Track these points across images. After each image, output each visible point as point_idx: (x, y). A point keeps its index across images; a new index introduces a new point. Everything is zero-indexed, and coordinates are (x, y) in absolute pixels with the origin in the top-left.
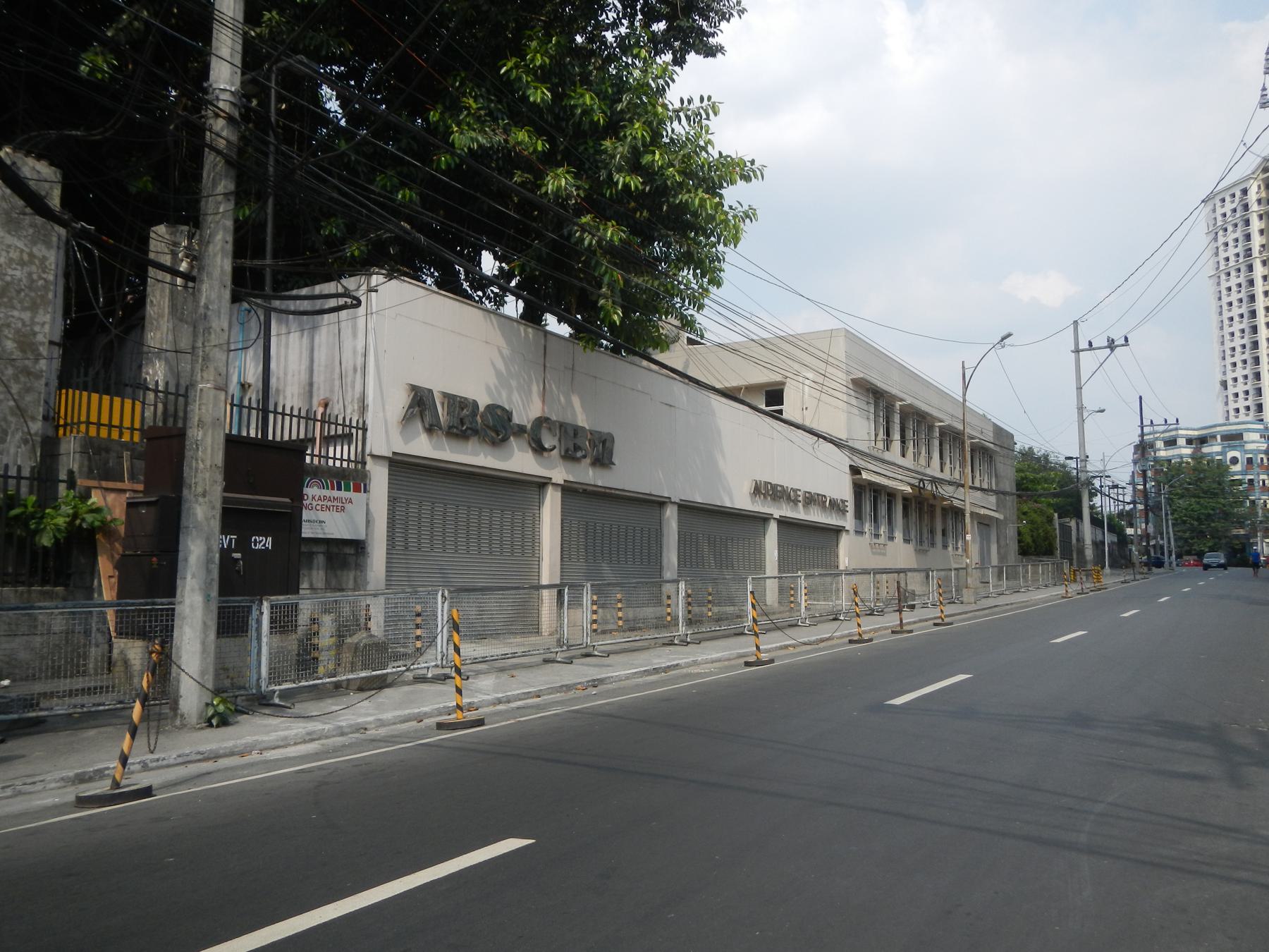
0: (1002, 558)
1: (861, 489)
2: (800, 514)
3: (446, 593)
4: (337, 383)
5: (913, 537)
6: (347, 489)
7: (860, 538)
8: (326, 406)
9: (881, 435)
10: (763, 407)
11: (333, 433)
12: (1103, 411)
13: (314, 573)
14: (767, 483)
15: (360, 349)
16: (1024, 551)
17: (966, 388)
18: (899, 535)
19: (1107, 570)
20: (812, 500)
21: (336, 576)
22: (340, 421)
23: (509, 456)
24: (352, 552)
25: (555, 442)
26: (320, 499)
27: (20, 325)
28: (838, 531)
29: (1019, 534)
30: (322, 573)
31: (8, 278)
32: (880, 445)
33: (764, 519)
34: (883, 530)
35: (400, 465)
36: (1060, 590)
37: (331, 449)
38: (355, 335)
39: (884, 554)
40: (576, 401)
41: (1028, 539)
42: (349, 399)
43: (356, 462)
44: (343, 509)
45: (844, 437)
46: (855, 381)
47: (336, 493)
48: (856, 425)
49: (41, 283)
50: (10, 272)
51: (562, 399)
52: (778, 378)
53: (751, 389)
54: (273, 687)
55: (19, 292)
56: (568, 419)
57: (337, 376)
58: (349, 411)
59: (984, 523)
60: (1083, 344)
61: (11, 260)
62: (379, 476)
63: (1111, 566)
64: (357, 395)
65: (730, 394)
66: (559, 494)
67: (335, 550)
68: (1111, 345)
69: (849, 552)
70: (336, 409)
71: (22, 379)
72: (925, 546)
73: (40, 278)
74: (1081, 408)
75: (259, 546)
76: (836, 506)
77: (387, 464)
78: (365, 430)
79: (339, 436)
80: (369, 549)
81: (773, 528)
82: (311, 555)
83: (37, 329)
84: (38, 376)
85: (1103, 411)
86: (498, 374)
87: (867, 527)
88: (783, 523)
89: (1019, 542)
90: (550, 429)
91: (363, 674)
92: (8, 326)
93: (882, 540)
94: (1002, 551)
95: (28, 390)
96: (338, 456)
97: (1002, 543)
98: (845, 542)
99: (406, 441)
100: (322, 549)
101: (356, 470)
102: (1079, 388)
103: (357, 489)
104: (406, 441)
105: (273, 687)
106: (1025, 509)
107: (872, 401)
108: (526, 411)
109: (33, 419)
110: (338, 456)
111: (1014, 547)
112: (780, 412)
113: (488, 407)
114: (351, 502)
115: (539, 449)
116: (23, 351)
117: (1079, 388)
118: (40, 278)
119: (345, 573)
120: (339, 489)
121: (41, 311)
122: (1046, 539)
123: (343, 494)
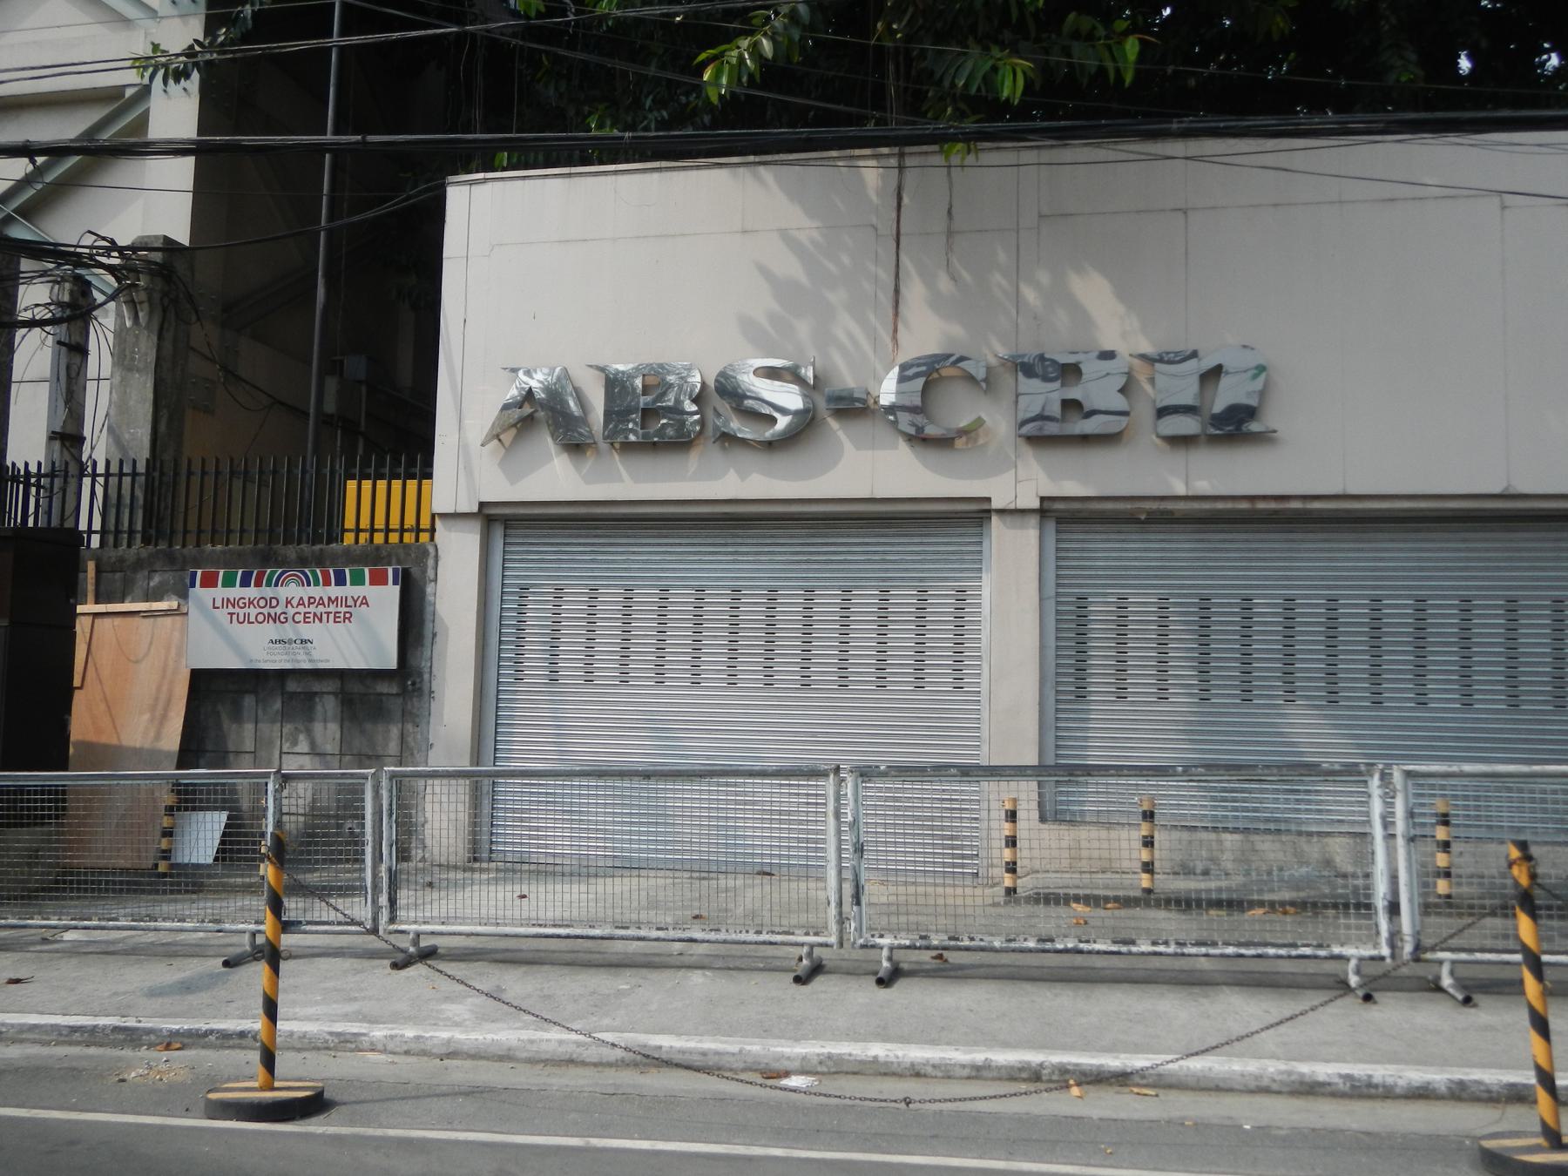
6: (358, 580)
13: (318, 727)
21: (363, 732)
24: (394, 690)
26: (301, 603)
30: (333, 728)
35: (500, 522)
44: (348, 618)
47: (334, 591)
67: (356, 687)
82: (310, 697)
86: (783, 289)
99: (514, 478)
100: (330, 686)
104: (514, 478)
114: (365, 602)
119: (380, 727)
120: (341, 581)
123: (349, 590)
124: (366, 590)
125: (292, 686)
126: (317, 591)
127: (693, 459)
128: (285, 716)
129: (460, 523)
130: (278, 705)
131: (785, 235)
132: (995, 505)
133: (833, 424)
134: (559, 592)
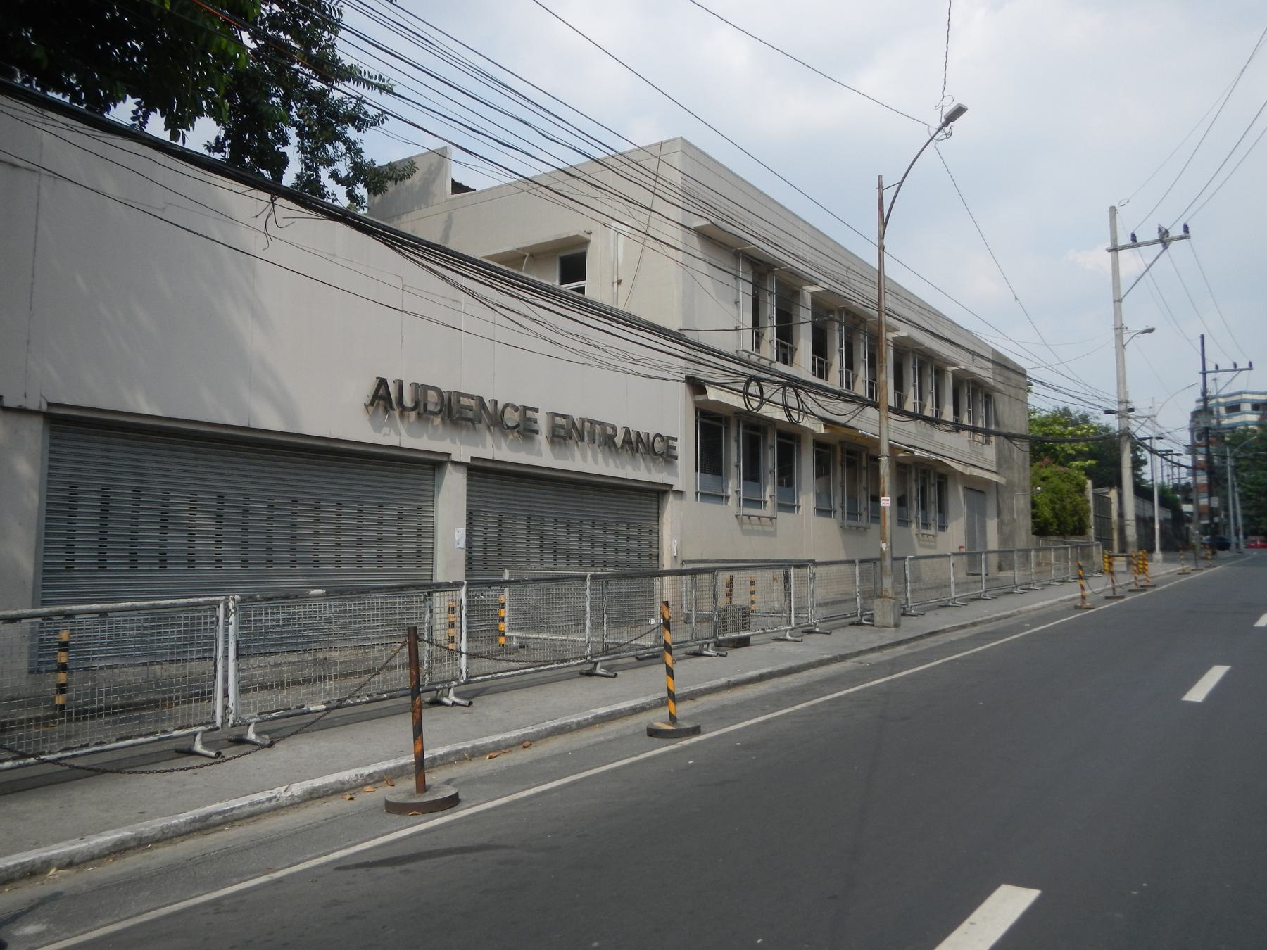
0: (1005, 538)
1: (711, 424)
2: (542, 456)
5: (837, 506)
9: (770, 334)
12: (1151, 331)
16: (1041, 529)
17: (884, 223)
18: (807, 500)
19: (1158, 555)
20: (566, 432)
28: (659, 493)
29: (1034, 505)
33: (435, 465)
34: (770, 491)
36: (1071, 592)
39: (773, 534)
41: (1047, 513)
46: (699, 232)
48: (721, 314)
59: (977, 490)
60: (1124, 240)
63: (1163, 549)
68: (1164, 239)
69: (690, 527)
72: (863, 522)
74: (1120, 329)
76: (663, 452)
81: (453, 487)
85: (1151, 331)
87: (733, 485)
88: (478, 471)
89: (1034, 516)
93: (769, 509)
94: (1006, 529)
97: (1006, 517)
102: (1118, 301)
106: (1046, 472)
111: (1025, 523)
112: (581, 290)
117: (1118, 301)
122: (1075, 513)
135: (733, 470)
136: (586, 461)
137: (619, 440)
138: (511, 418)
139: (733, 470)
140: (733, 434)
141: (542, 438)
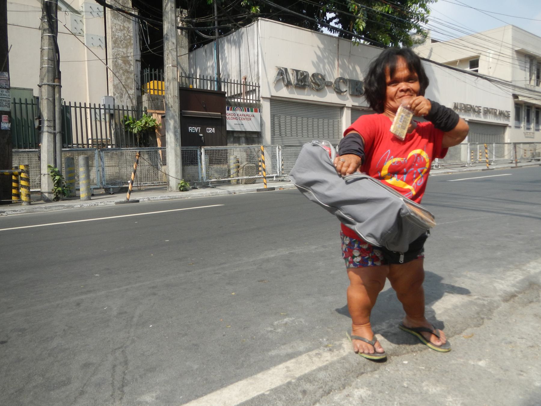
1: (518, 106)
2: (481, 118)
3: (280, 147)
4: (249, 69)
6: (252, 111)
7: (517, 130)
8: (245, 79)
10: (468, 69)
11: (248, 90)
14: (461, 104)
15: (256, 54)
20: (487, 111)
22: (251, 84)
23: (325, 95)
25: (347, 89)
26: (240, 115)
27: (123, 54)
28: (504, 127)
31: (117, 36)
32: (533, 83)
34: (532, 126)
35: (275, 101)
37: (248, 97)
38: (254, 48)
40: (358, 69)
42: (253, 75)
43: (256, 100)
45: (509, 79)
49: (128, 37)
50: (117, 34)
51: (351, 68)
52: (473, 54)
53: (462, 61)
54: (208, 180)
55: (121, 41)
56: (354, 78)
57: (249, 66)
58: (253, 80)
61: (117, 29)
62: (266, 106)
64: (256, 73)
65: (448, 66)
66: (350, 111)
67: (248, 136)
70: (249, 80)
71: (126, 74)
73: (128, 35)
75: (210, 132)
76: (503, 115)
77: (269, 100)
78: (259, 87)
79: (251, 91)
80: (263, 136)
82: (239, 138)
83: (129, 55)
84: (131, 73)
90: (344, 82)
91: (245, 177)
92: (119, 54)
93: (532, 130)
95: (128, 78)
96: (251, 98)
98: (508, 131)
99: (277, 91)
100: (243, 135)
101: (256, 104)
103: (256, 111)
104: (277, 91)
105: (208, 180)
107: (529, 60)
108: (333, 74)
109: (131, 89)
110: (251, 98)
112: (477, 71)
113: (313, 75)
115: (339, 92)
116: (125, 64)
118: (128, 35)
120: (248, 111)
121: (129, 48)
123: (250, 113)
124: (254, 113)
125: (235, 135)
126: (244, 113)
127: (307, 90)
128: (234, 142)
129: (266, 100)
130: (232, 140)
131: (319, 47)
132: (347, 106)
133: (326, 87)
134: (280, 117)
135: (523, 119)
136: (491, 119)
137: (498, 113)
138: (477, 109)
139: (523, 119)
140: (523, 109)
141: (482, 114)
